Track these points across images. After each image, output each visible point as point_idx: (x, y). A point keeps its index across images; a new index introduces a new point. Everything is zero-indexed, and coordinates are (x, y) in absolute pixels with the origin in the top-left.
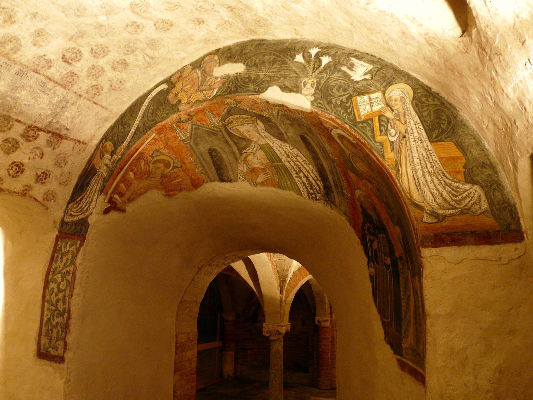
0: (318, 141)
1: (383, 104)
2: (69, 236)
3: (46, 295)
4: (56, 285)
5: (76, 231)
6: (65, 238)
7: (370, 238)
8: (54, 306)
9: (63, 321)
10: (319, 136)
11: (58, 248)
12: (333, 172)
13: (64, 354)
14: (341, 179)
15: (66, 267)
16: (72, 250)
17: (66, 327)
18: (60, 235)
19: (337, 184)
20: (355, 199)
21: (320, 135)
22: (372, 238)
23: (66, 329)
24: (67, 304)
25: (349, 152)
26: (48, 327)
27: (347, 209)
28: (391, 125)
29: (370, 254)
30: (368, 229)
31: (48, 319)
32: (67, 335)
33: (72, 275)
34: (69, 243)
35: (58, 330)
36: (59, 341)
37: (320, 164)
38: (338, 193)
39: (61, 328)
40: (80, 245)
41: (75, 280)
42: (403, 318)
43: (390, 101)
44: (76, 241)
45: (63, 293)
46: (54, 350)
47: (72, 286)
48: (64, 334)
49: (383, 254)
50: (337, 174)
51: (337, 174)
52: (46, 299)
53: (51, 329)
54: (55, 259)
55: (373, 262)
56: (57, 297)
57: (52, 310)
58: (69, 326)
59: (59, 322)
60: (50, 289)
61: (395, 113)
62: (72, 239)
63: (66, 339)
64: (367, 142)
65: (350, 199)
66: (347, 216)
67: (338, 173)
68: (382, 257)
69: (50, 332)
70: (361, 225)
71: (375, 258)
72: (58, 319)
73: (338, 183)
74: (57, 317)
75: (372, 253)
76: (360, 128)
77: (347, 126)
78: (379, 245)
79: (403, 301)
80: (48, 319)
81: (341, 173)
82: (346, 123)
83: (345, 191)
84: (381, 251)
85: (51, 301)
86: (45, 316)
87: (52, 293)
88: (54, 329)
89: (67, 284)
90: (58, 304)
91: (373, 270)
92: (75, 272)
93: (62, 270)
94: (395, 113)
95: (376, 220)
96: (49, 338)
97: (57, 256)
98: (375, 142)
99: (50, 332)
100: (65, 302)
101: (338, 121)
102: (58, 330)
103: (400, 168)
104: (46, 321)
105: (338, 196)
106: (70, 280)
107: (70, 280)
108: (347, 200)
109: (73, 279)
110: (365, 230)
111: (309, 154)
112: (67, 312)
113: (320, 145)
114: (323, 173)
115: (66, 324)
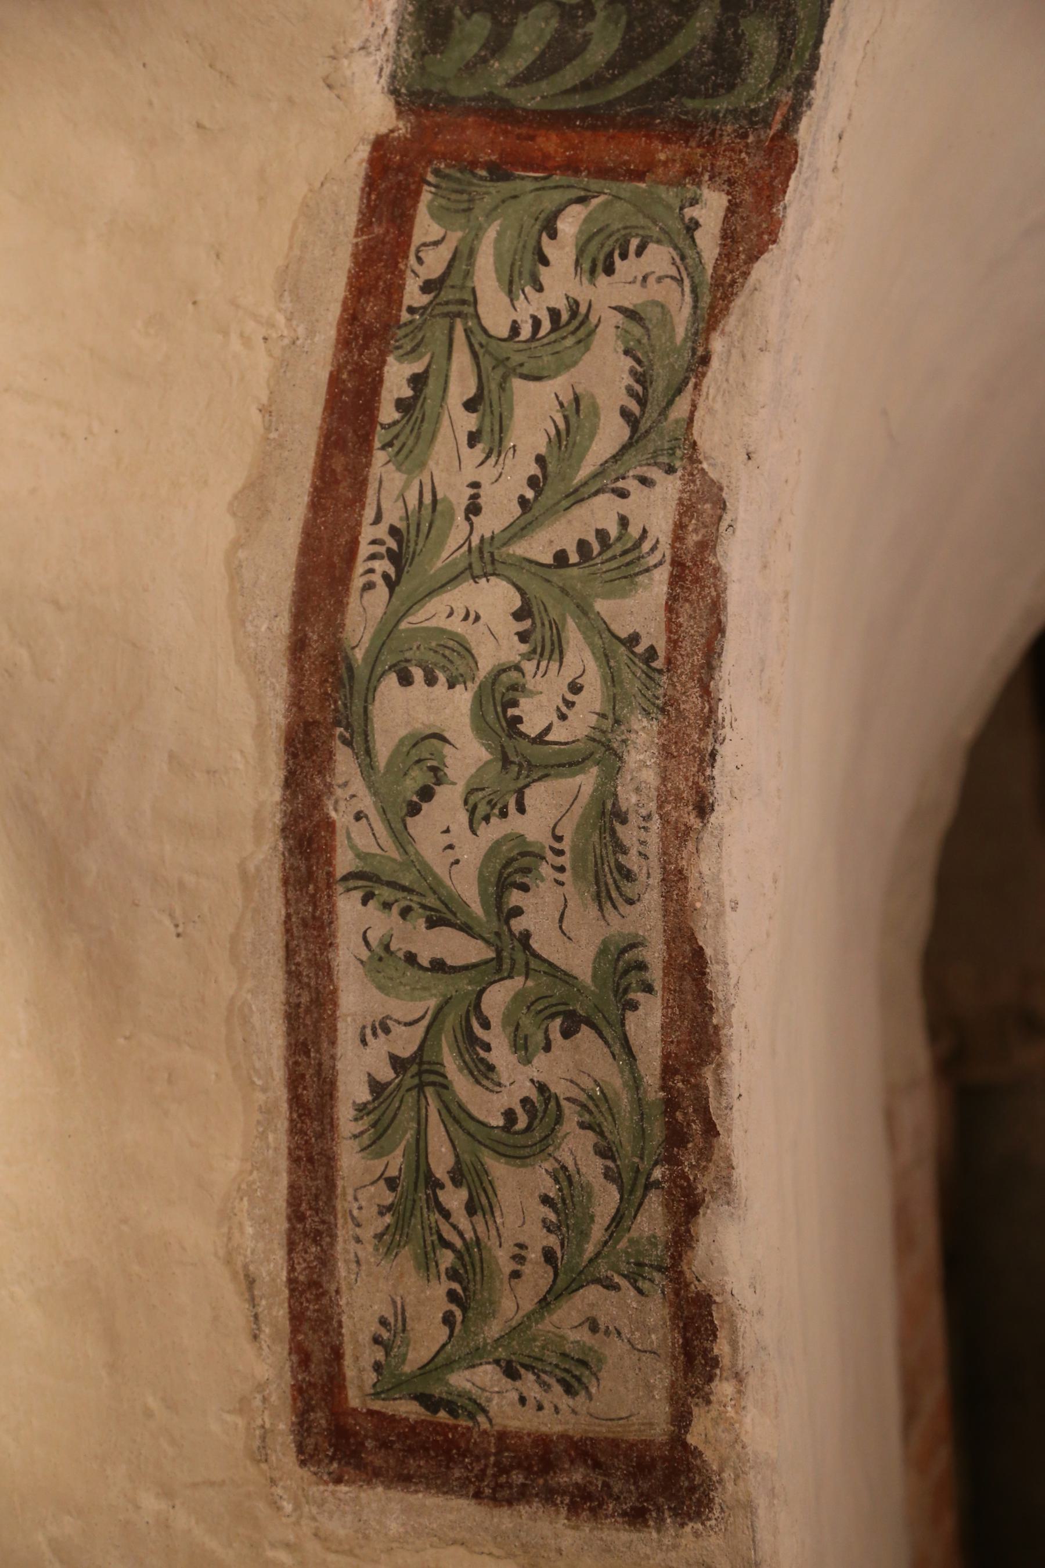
2: (549, 143)
3: (341, 817)
4: (463, 698)
5: (652, 69)
6: (498, 172)
8: (466, 929)
9: (615, 1080)
11: (413, 295)
13: (682, 1419)
15: (577, 496)
16: (632, 297)
17: (676, 1137)
18: (419, 132)
23: (671, 1160)
24: (652, 898)
26: (420, 1147)
31: (397, 1063)
32: (703, 1226)
33: (675, 580)
34: (569, 225)
35: (563, 1175)
36: (592, 1293)
39: (605, 1152)
40: (728, 237)
41: (719, 629)
44: (669, 195)
45: (587, 781)
46: (529, 1383)
47: (692, 703)
48: (654, 1203)
52: (344, 862)
53: (457, 1177)
54: (388, 413)
56: (494, 830)
57: (438, 966)
58: (711, 1130)
59: (559, 1089)
60: (383, 749)
62: (603, 172)
63: (697, 1260)
69: (454, 1199)
72: (541, 1060)
74: (521, 1046)
80: (397, 1063)
85: (425, 871)
86: (347, 1032)
87: (427, 793)
88: (498, 1169)
89: (612, 679)
90: (515, 898)
92: (707, 546)
93: (519, 530)
96: (447, 1259)
97: (418, 381)
99: (454, 1199)
100: (628, 875)
102: (563, 1175)
104: (377, 1087)
106: (654, 636)
107: (654, 636)
109: (692, 627)
112: (656, 975)
115: (671, 1105)
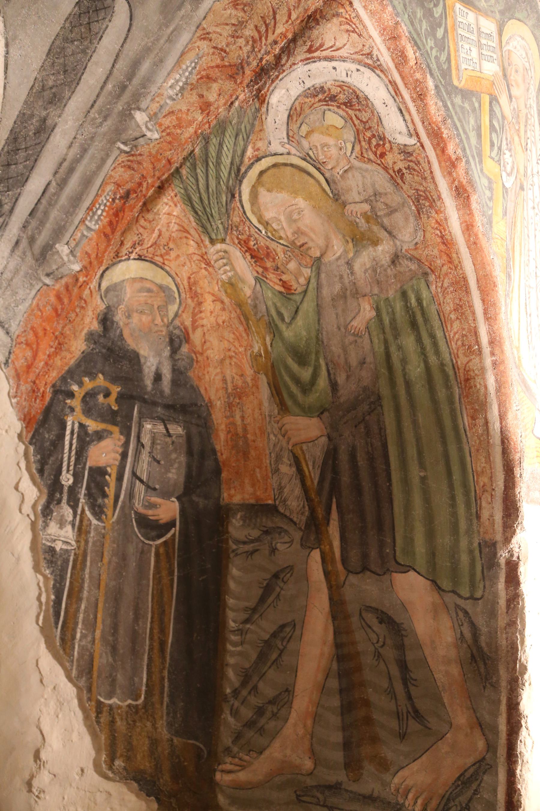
0: (148, 50)
1: (499, 65)
7: (82, 426)
10: (185, 38)
12: (71, 170)
14: (87, 203)
19: (46, 213)
20: (94, 285)
21: (206, 37)
22: (92, 425)
25: (276, 147)
27: (23, 308)
28: (507, 139)
29: (67, 479)
30: (90, 396)
37: (44, 120)
38: (17, 243)
42: (228, 691)
43: (509, 65)
49: (139, 488)
50: (87, 182)
51: (87, 182)
55: (74, 508)
61: (514, 109)
64: (468, 162)
65: (63, 281)
66: (8, 333)
67: (98, 182)
68: (131, 495)
70: (54, 375)
71: (89, 495)
73: (54, 214)
75: (78, 477)
76: (458, 109)
77: (430, 84)
78: (124, 455)
79: (234, 638)
81: (110, 188)
82: (432, 75)
83: (63, 249)
84: (134, 474)
91: (68, 533)
94: (514, 109)
95: (158, 377)
98: (482, 170)
101: (410, 53)
103: (512, 274)
105: (13, 251)
108: (47, 281)
110: (71, 395)
111: (36, 65)
113: (136, 64)
114: (22, 154)
